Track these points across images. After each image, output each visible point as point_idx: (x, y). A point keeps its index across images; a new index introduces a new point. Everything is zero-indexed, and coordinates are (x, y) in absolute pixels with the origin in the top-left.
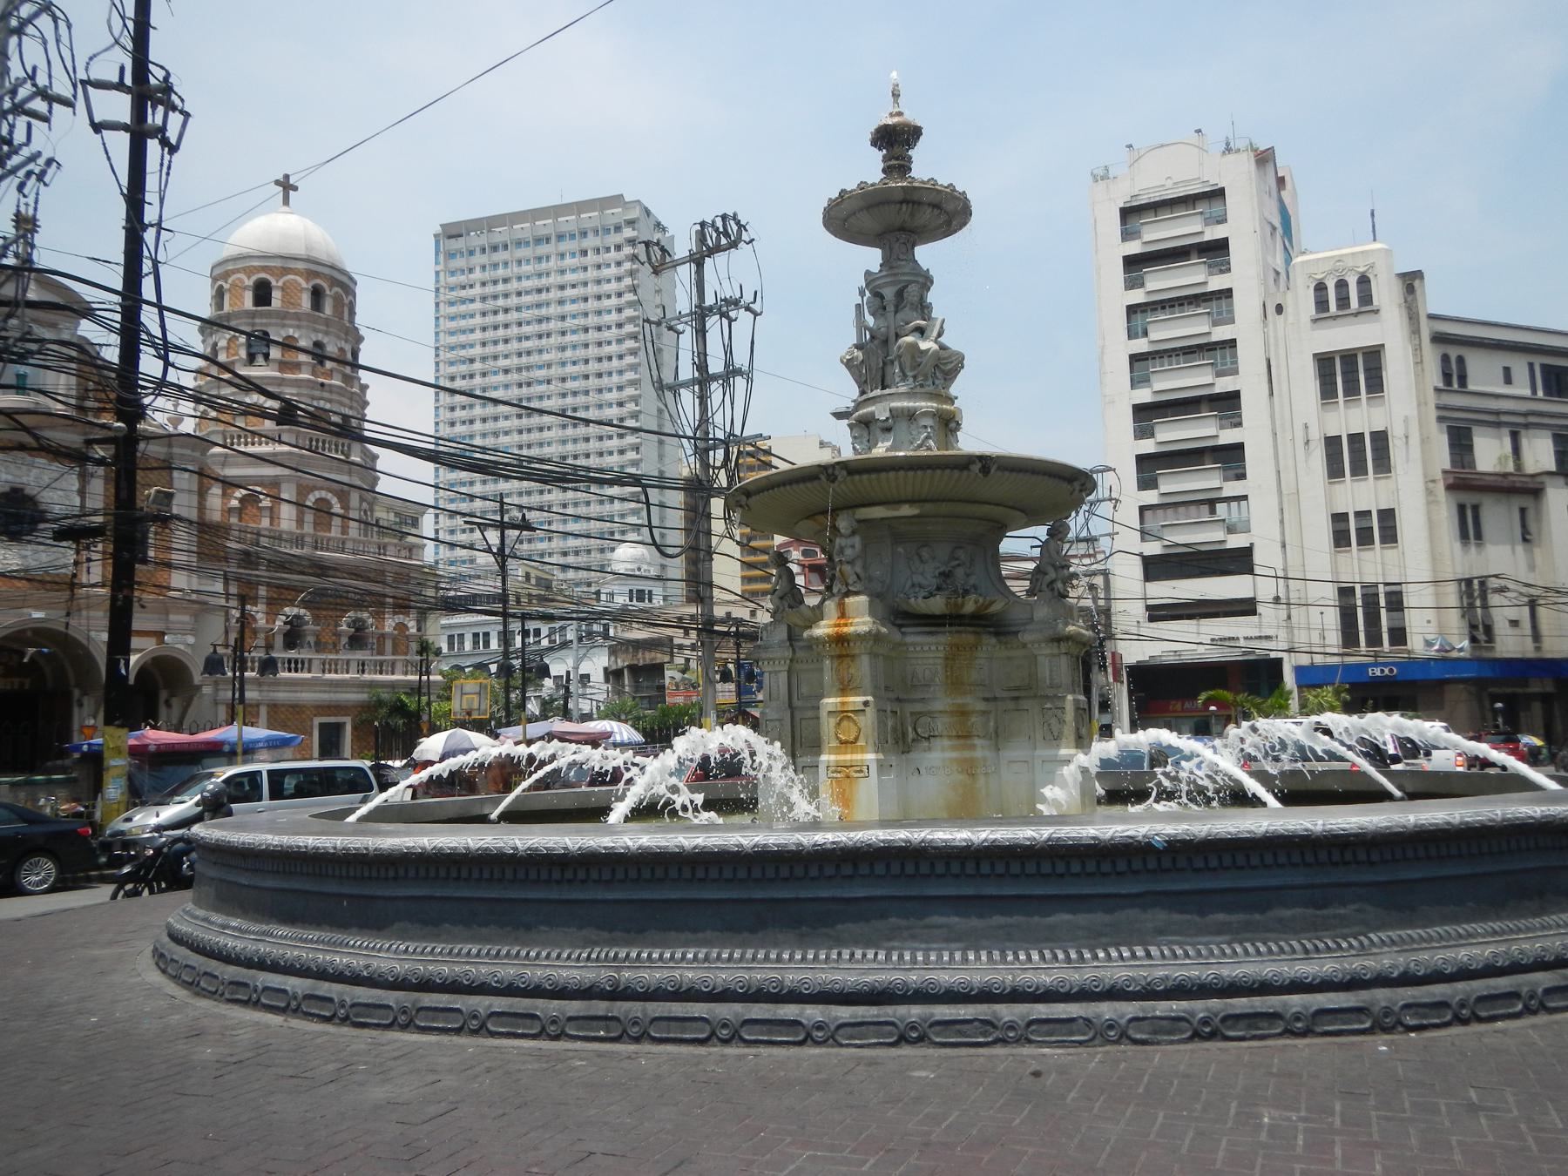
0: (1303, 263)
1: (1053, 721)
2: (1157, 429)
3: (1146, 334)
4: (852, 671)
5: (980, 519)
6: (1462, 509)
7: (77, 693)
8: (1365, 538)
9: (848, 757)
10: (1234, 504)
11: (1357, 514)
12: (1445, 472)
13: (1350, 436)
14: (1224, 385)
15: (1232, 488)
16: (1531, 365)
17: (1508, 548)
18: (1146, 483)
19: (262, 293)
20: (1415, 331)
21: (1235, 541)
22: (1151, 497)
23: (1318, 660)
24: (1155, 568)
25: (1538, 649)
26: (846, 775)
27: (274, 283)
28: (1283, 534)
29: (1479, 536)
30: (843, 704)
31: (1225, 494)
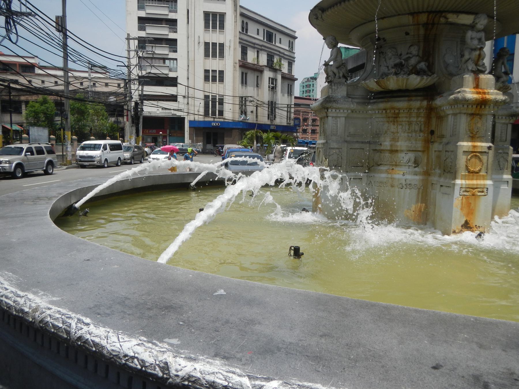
1: (501, 160)
2: (147, 28)
4: (479, 125)
6: (242, 73)
8: (214, 80)
9: (475, 182)
10: (172, 61)
11: (212, 70)
12: (239, 61)
14: (172, 16)
15: (172, 55)
16: (264, 30)
17: (252, 88)
20: (236, 10)
21: (172, 75)
24: (144, 81)
25: (257, 120)
26: (472, 194)
28: (188, 74)
29: (246, 84)
30: (474, 147)
31: (169, 57)
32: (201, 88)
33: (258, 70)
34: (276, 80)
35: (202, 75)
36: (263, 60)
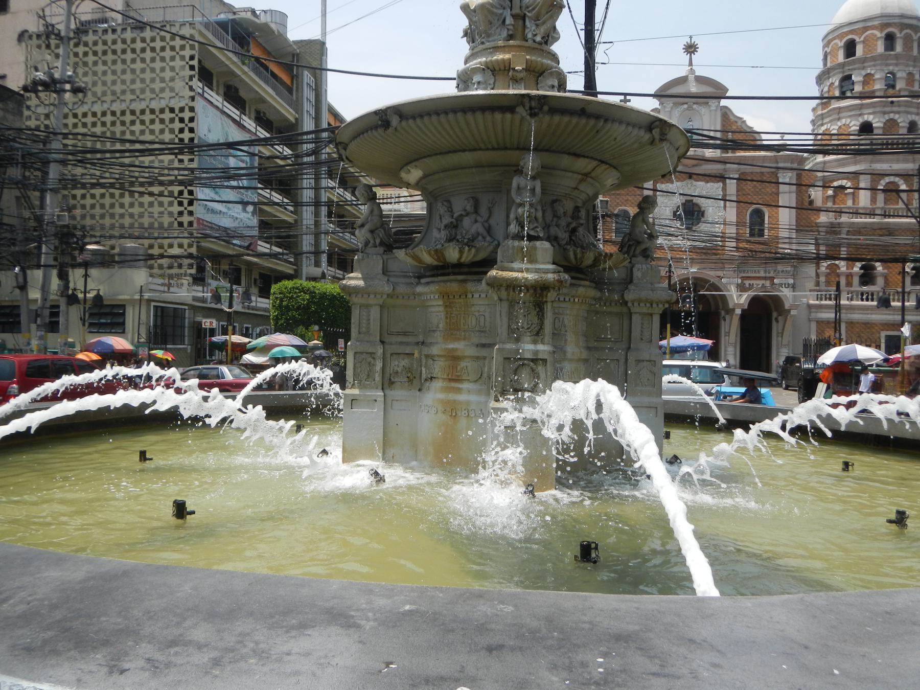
5: (490, 166)
7: (723, 313)
19: (850, 49)
27: (857, 40)
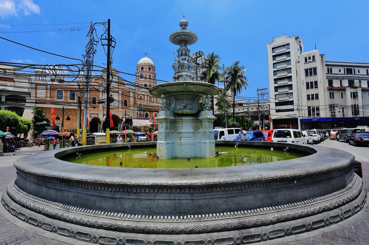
0: (303, 54)
3: (276, 68)
6: (330, 93)
7: (119, 123)
8: (313, 98)
13: (310, 82)
14: (289, 75)
15: (290, 91)
16: (344, 69)
18: (276, 91)
19: (142, 68)
22: (277, 93)
23: (304, 118)
28: (298, 98)
29: (333, 98)
32: (305, 103)
33: (342, 89)
34: (357, 93)
35: (306, 98)
36: (346, 83)
